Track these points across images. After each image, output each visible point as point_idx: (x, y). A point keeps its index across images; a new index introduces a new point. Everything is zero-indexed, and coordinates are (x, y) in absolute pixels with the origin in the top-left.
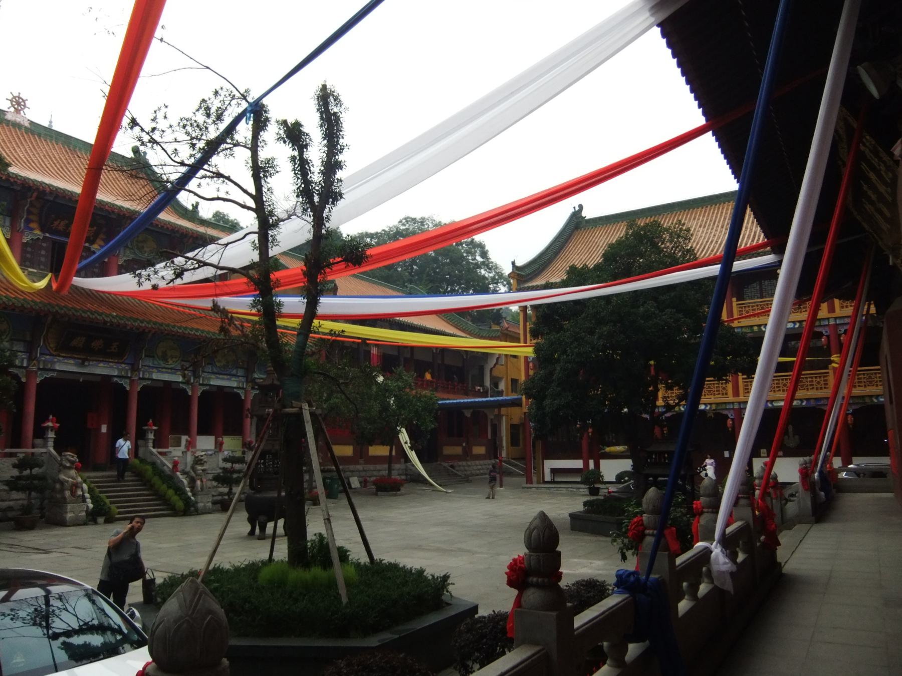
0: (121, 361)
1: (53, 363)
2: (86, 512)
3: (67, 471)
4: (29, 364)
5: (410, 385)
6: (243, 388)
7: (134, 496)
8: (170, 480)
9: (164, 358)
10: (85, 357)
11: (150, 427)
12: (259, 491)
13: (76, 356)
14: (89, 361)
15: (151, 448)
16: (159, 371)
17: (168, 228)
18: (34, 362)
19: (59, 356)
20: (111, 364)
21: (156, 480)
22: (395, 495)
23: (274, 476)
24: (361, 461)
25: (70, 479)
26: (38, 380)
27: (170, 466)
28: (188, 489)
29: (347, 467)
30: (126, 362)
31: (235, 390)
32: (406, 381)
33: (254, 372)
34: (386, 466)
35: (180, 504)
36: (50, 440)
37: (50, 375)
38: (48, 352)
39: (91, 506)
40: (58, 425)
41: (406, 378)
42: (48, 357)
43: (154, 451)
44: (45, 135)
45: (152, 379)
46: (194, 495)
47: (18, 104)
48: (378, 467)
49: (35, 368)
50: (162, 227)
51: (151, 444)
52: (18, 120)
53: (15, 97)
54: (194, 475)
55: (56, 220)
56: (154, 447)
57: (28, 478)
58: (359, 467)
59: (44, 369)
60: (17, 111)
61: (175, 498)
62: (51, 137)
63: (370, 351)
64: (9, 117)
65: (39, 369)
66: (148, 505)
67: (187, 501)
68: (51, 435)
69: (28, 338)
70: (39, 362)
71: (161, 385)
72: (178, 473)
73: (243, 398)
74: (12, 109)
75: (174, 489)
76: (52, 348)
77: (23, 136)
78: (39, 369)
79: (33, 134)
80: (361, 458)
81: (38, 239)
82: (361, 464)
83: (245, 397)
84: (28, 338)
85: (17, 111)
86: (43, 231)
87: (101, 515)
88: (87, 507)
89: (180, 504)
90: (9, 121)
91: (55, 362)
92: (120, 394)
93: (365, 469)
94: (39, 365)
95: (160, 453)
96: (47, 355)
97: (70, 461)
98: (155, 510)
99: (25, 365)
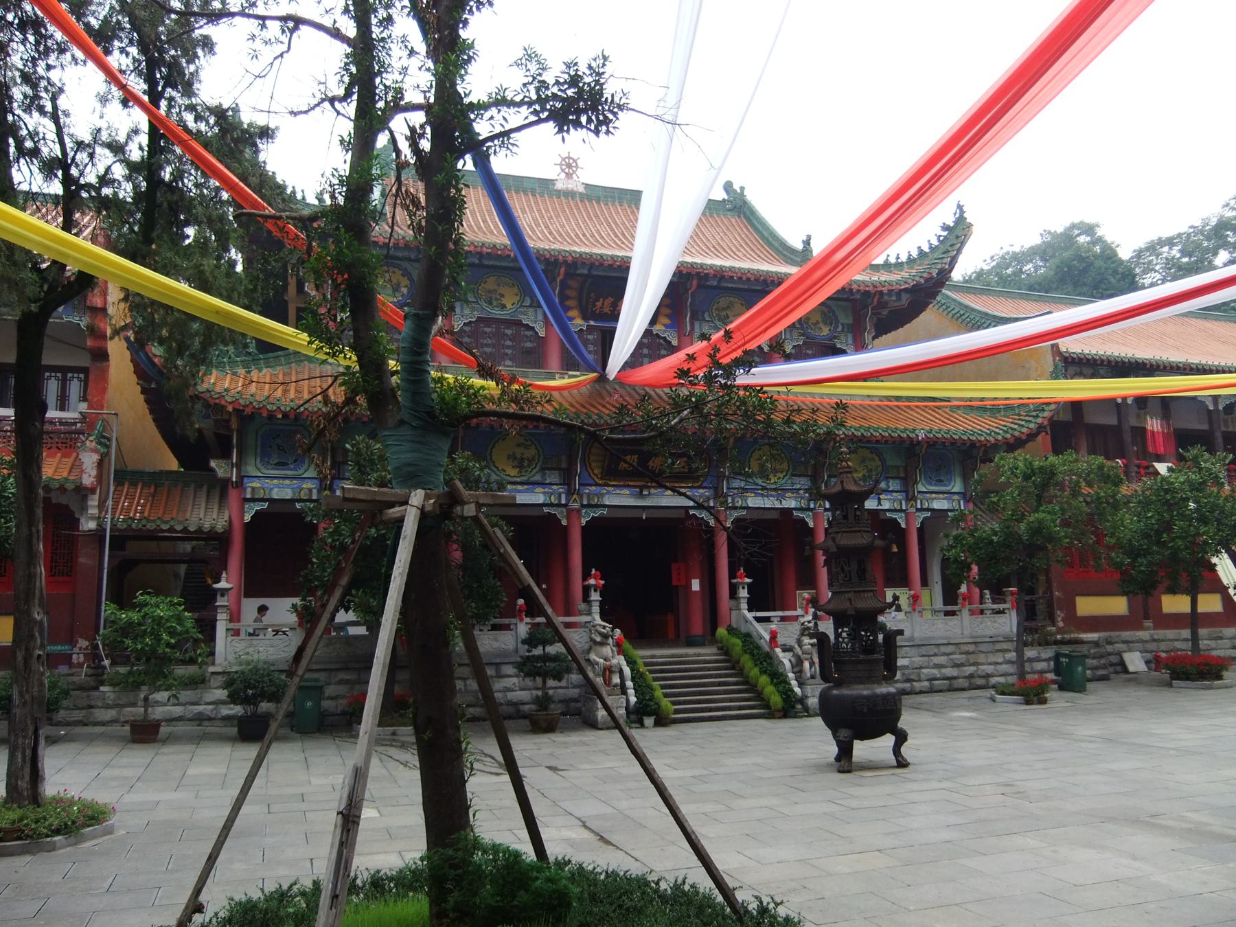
0: (697, 485)
1: (601, 496)
2: (627, 708)
3: (598, 648)
4: (568, 500)
5: (1217, 477)
6: (901, 510)
7: (713, 684)
8: (766, 661)
9: (764, 474)
10: (642, 483)
11: (739, 580)
12: (839, 684)
13: (631, 483)
14: (649, 488)
15: (746, 612)
16: (757, 495)
17: (748, 279)
18: (575, 496)
21: (746, 661)
22: (1209, 688)
23: (862, 657)
24: (1149, 623)
25: (602, 661)
26: (584, 522)
27: (767, 637)
28: (791, 675)
29: (1117, 633)
30: (705, 485)
31: (888, 514)
32: (1208, 470)
33: (916, 482)
34: (1186, 633)
35: (776, 700)
36: (594, 604)
37: (599, 513)
38: (592, 482)
39: (633, 699)
40: (602, 582)
41: (1208, 465)
42: (593, 488)
43: (750, 616)
44: (606, 197)
45: (748, 508)
46: (801, 685)
47: (569, 166)
48: (1170, 634)
49: (576, 505)
50: (740, 278)
51: (744, 606)
52: (570, 186)
53: (563, 159)
54: (800, 653)
55: (599, 300)
56: (750, 610)
57: (538, 658)
58: (1144, 635)
59: (589, 506)
60: (569, 176)
61: (770, 690)
62: (613, 197)
63: (1144, 430)
64: (559, 186)
65: (583, 506)
66: (731, 700)
67: (787, 694)
68: (595, 596)
69: (564, 465)
70: (581, 496)
71: (775, 515)
72: (778, 650)
73: (903, 526)
74: (563, 175)
75: (770, 675)
76: (597, 476)
77: (577, 206)
78: (583, 506)
79: (590, 200)
80: (1147, 617)
81: (581, 330)
82: (1148, 629)
83: (907, 523)
84: (564, 465)
85: (569, 176)
86: (585, 318)
87: (649, 714)
88: (628, 701)
89: (776, 700)
90: (559, 191)
91: (604, 494)
92: (709, 534)
93: (1155, 637)
94: (581, 500)
95: (758, 619)
96: (591, 485)
97: (601, 634)
98: (740, 708)
99: (563, 502)
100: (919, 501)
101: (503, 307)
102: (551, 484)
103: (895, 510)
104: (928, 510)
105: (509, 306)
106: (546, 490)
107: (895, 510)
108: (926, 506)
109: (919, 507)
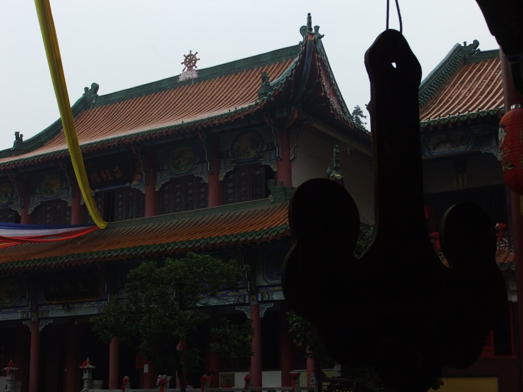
19: (53, 304)
20: (93, 303)
42: (45, 307)
59: (42, 319)
78: (39, 319)
96: (43, 305)
99: (29, 317)
100: (260, 295)
101: (52, 192)
102: (24, 306)
103: (240, 305)
104: (269, 301)
105: (55, 191)
106: (23, 310)
107: (240, 305)
108: (266, 298)
109: (260, 299)
